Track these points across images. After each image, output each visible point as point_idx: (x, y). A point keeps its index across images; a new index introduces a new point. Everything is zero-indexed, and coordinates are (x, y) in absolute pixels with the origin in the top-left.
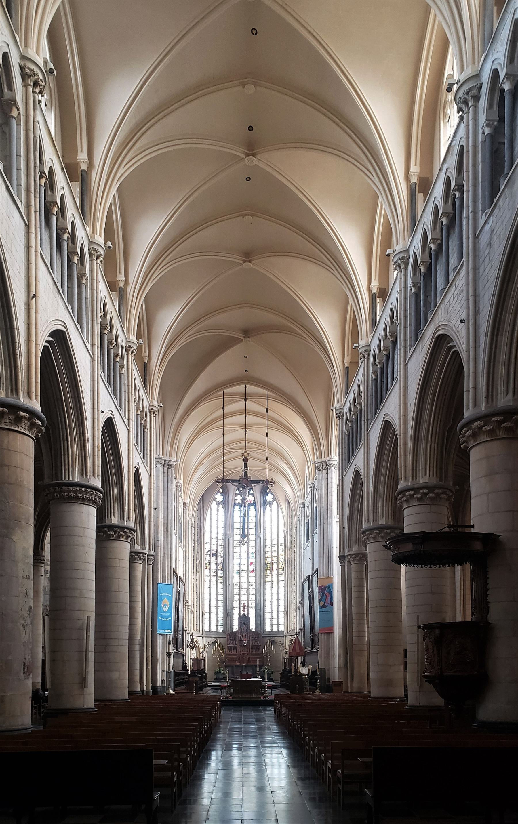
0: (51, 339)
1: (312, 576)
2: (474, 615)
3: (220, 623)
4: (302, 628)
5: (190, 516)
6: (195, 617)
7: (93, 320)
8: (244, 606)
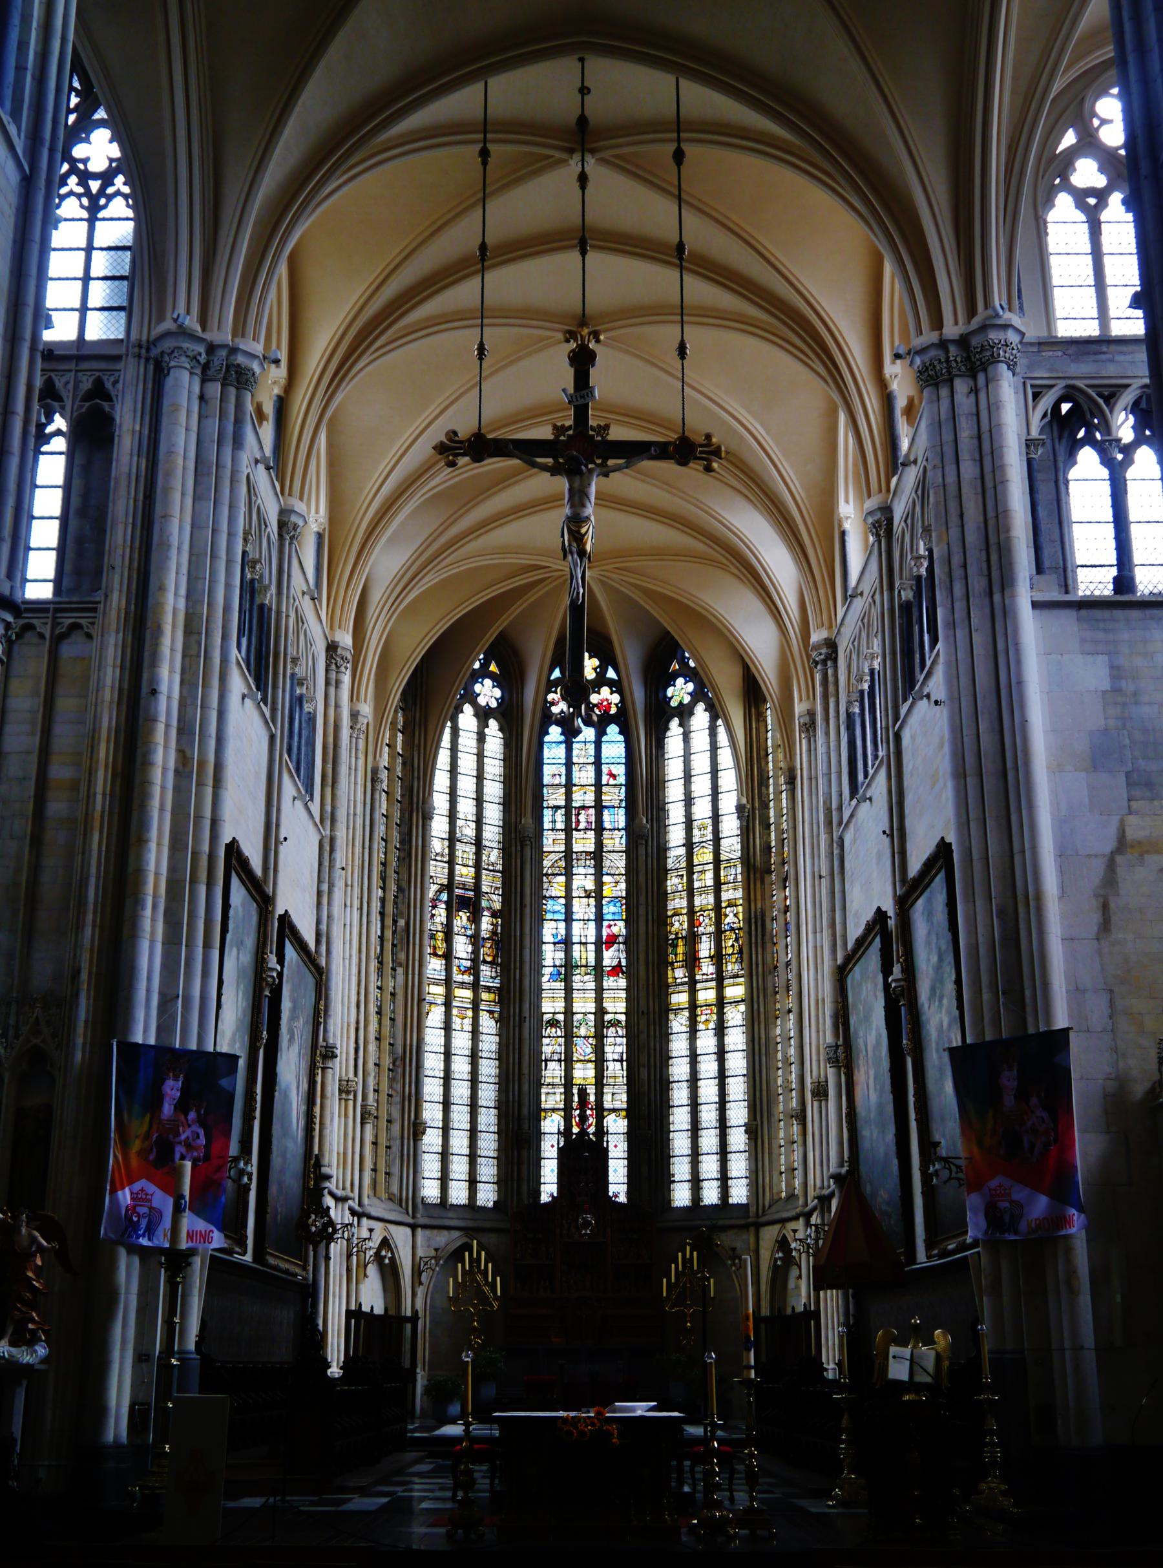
3: (487, 1170)
6: (383, 1141)
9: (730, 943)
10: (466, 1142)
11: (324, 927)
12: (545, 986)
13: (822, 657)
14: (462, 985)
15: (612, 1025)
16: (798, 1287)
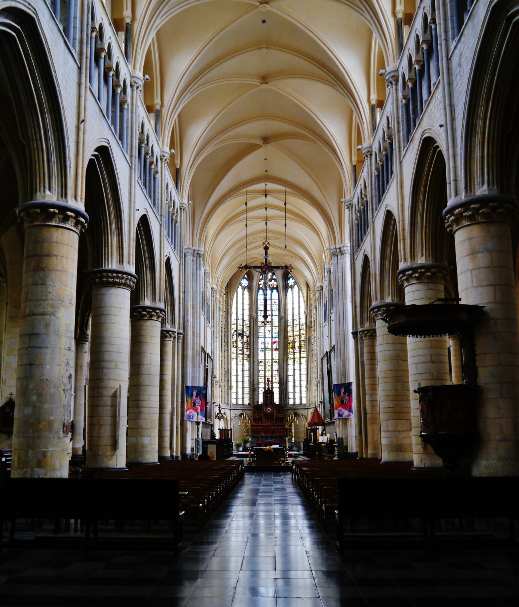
0: (96, 153)
1: (330, 352)
2: (465, 379)
3: (247, 396)
4: (322, 400)
5: (218, 299)
6: (223, 391)
7: (132, 137)
8: (268, 381)
9: (302, 344)
11: (213, 350)
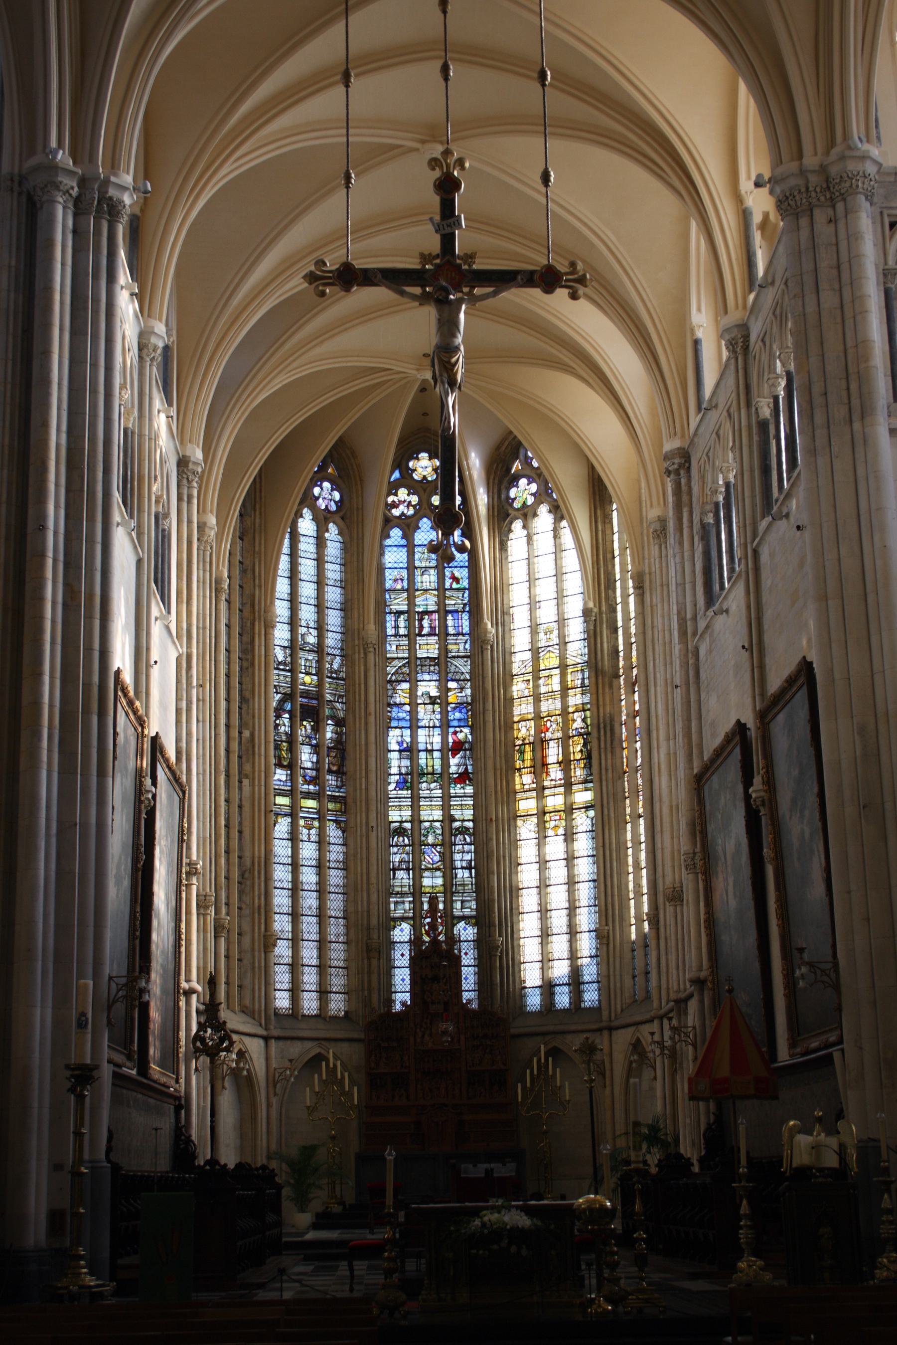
3: (337, 981)
9: (579, 748)
10: (315, 953)
12: (393, 794)
13: (676, 466)
14: (308, 795)
15: (460, 833)
16: (652, 1089)
